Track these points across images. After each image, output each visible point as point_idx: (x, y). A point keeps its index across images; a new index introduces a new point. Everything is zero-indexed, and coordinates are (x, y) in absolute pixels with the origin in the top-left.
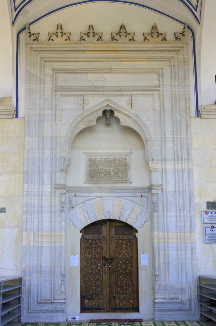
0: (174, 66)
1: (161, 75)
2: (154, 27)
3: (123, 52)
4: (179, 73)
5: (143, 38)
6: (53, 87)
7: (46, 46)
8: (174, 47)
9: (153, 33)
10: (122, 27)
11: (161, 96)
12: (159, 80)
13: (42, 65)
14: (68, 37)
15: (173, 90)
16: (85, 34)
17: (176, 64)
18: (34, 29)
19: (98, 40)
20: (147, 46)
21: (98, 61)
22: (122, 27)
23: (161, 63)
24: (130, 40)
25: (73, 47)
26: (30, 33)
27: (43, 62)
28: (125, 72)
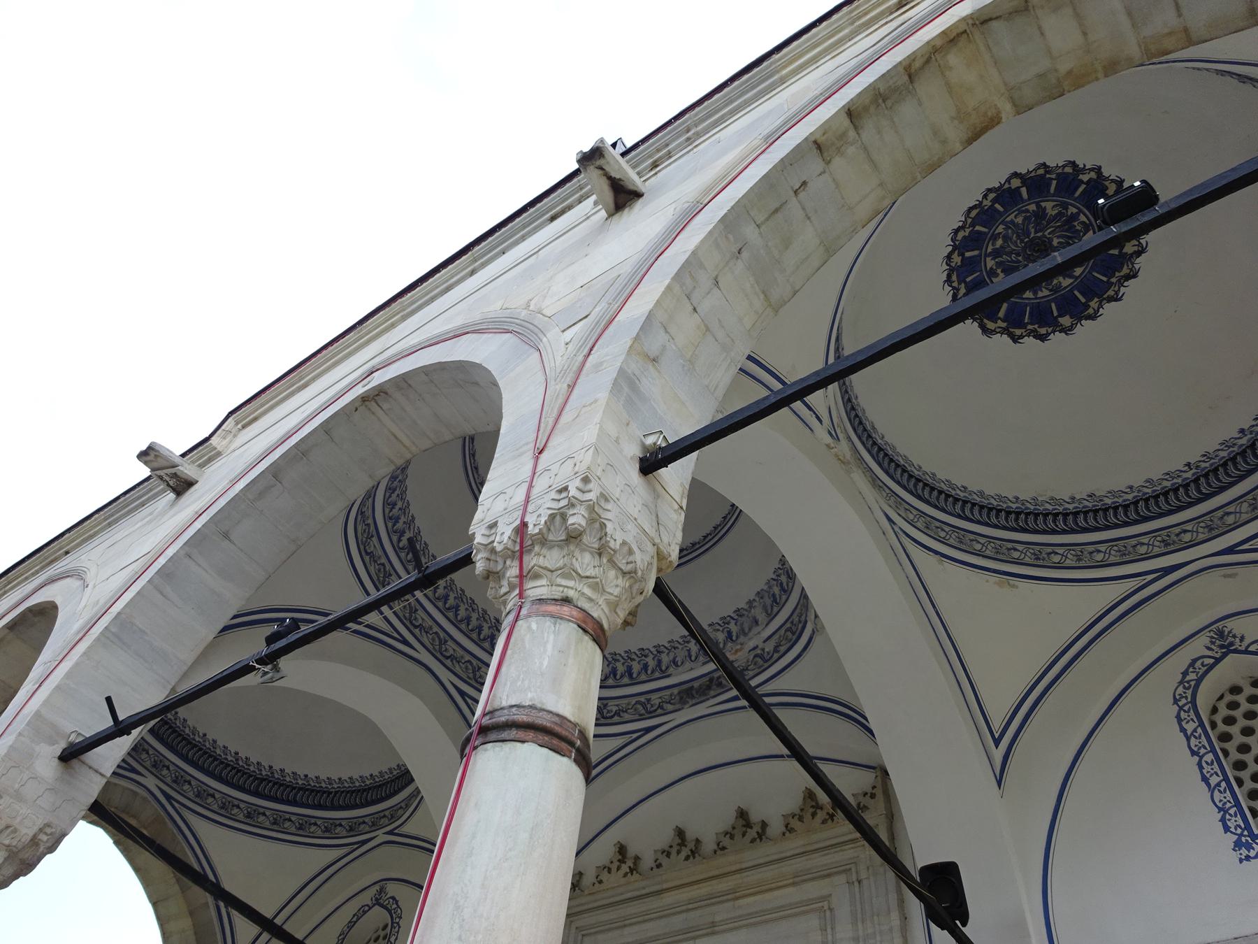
1: (828, 913)
10: (742, 814)
20: (794, 844)
22: (742, 814)
23: (827, 880)
24: (753, 841)
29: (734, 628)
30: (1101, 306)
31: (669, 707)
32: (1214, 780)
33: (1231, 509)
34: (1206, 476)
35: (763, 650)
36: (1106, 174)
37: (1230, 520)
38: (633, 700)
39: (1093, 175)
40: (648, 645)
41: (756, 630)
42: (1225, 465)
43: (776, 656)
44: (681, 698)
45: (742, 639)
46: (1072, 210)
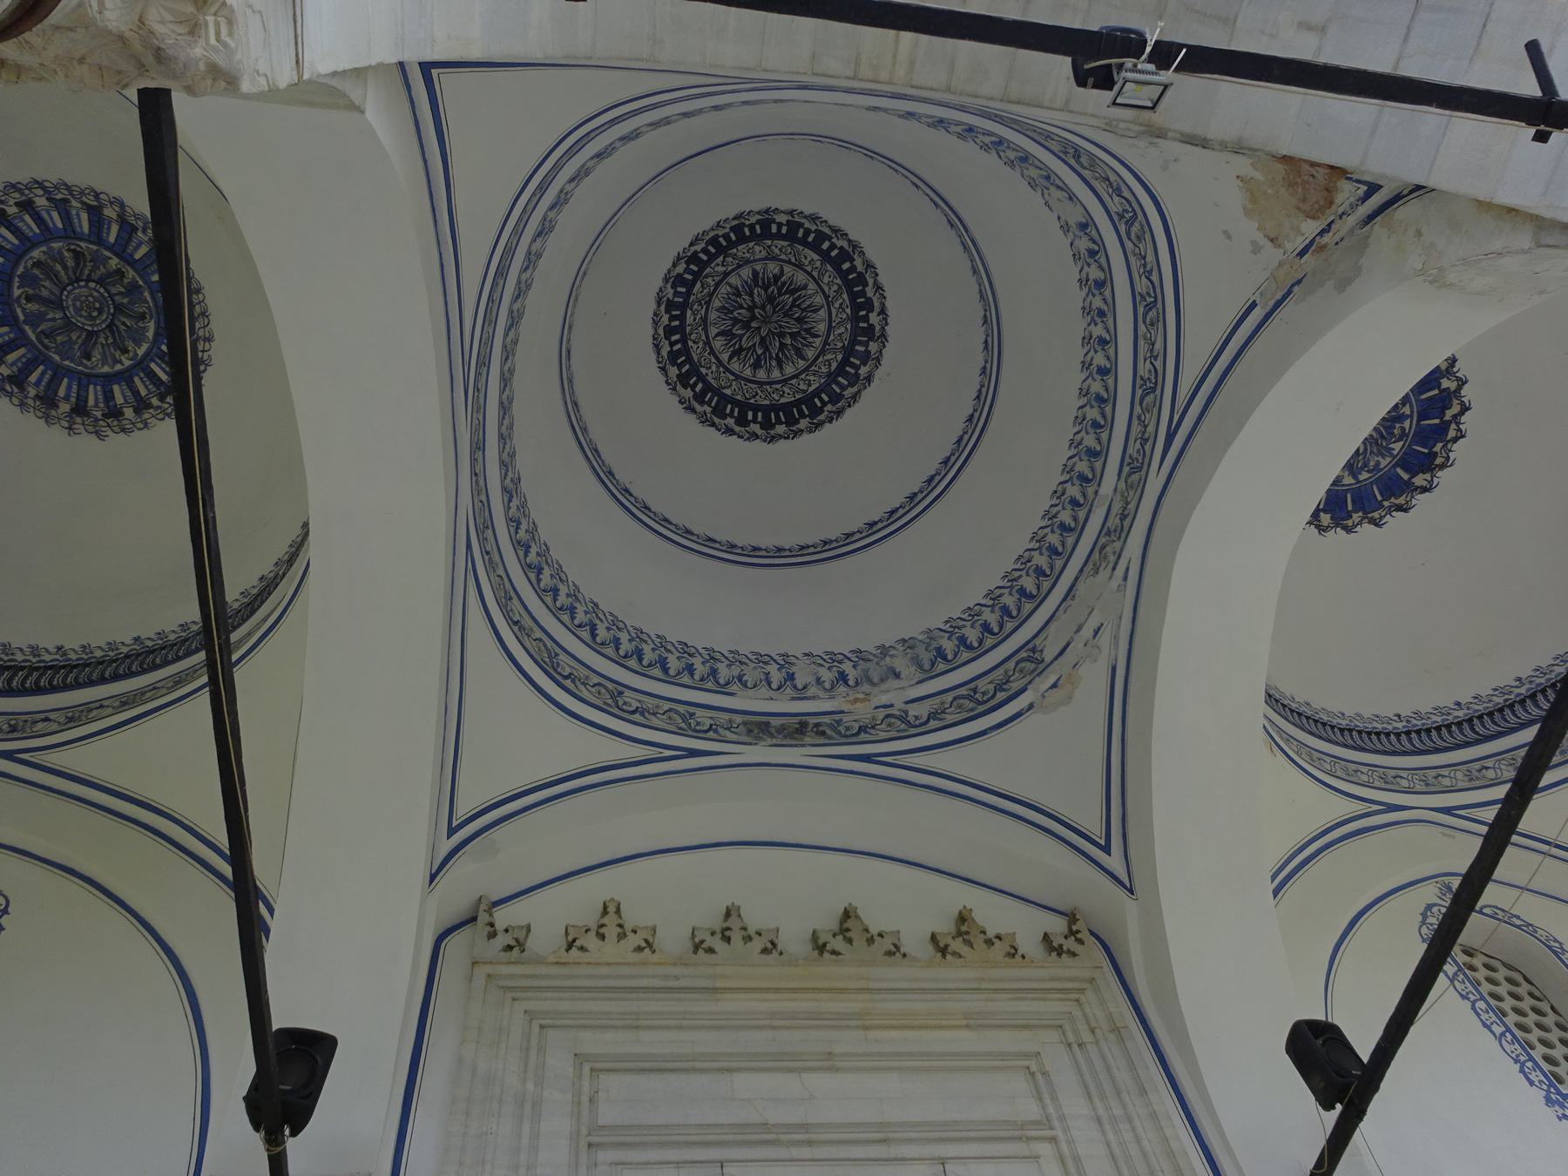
0: (1080, 1045)
1: (1039, 1076)
2: (963, 918)
3: (866, 996)
4: (1108, 1069)
5: (931, 949)
6: (578, 1131)
7: (555, 970)
8: (1059, 979)
9: (967, 933)
11: (1070, 1163)
12: (1041, 1099)
13: (534, 1042)
14: (646, 941)
15: (1111, 1136)
16: (713, 934)
17: (1086, 1037)
18: (503, 917)
19: (765, 951)
21: (773, 1028)
24: (889, 953)
25: (666, 977)
26: (492, 925)
27: (536, 1029)
28: (889, 1069)
29: (847, 667)
30: (1360, 523)
31: (730, 736)
32: (1498, 1030)
33: (1445, 772)
34: (1418, 732)
35: (906, 712)
36: (1463, 393)
37: (1447, 782)
38: (666, 706)
39: (1453, 386)
40: (698, 642)
41: (893, 683)
42: (1438, 729)
43: (933, 724)
44: (750, 732)
45: (866, 687)
46: (1407, 410)
